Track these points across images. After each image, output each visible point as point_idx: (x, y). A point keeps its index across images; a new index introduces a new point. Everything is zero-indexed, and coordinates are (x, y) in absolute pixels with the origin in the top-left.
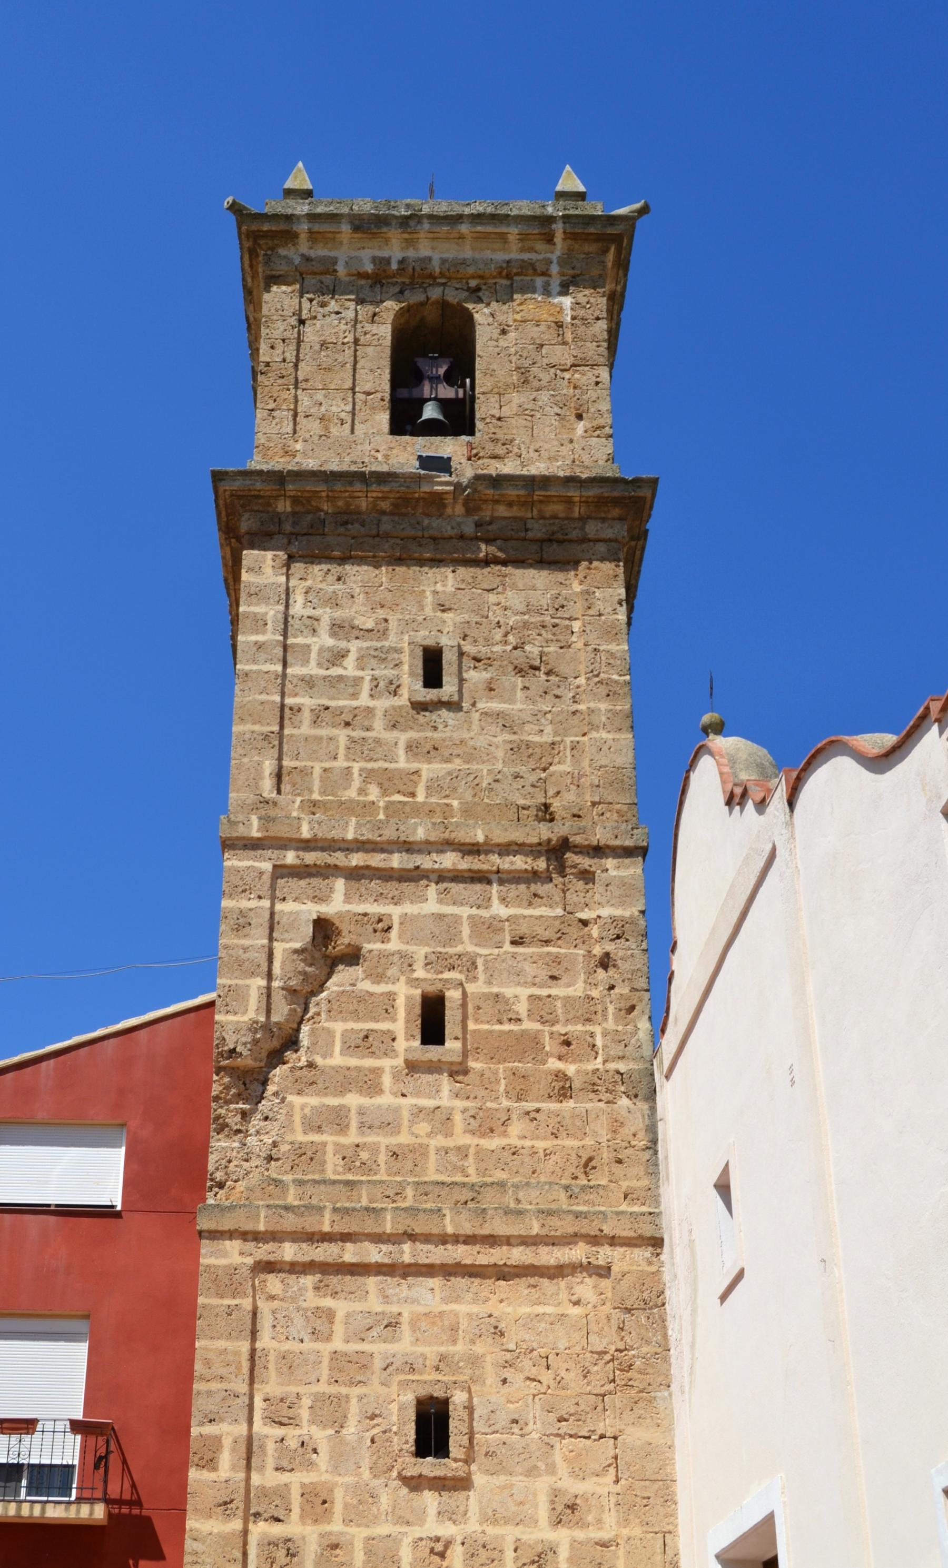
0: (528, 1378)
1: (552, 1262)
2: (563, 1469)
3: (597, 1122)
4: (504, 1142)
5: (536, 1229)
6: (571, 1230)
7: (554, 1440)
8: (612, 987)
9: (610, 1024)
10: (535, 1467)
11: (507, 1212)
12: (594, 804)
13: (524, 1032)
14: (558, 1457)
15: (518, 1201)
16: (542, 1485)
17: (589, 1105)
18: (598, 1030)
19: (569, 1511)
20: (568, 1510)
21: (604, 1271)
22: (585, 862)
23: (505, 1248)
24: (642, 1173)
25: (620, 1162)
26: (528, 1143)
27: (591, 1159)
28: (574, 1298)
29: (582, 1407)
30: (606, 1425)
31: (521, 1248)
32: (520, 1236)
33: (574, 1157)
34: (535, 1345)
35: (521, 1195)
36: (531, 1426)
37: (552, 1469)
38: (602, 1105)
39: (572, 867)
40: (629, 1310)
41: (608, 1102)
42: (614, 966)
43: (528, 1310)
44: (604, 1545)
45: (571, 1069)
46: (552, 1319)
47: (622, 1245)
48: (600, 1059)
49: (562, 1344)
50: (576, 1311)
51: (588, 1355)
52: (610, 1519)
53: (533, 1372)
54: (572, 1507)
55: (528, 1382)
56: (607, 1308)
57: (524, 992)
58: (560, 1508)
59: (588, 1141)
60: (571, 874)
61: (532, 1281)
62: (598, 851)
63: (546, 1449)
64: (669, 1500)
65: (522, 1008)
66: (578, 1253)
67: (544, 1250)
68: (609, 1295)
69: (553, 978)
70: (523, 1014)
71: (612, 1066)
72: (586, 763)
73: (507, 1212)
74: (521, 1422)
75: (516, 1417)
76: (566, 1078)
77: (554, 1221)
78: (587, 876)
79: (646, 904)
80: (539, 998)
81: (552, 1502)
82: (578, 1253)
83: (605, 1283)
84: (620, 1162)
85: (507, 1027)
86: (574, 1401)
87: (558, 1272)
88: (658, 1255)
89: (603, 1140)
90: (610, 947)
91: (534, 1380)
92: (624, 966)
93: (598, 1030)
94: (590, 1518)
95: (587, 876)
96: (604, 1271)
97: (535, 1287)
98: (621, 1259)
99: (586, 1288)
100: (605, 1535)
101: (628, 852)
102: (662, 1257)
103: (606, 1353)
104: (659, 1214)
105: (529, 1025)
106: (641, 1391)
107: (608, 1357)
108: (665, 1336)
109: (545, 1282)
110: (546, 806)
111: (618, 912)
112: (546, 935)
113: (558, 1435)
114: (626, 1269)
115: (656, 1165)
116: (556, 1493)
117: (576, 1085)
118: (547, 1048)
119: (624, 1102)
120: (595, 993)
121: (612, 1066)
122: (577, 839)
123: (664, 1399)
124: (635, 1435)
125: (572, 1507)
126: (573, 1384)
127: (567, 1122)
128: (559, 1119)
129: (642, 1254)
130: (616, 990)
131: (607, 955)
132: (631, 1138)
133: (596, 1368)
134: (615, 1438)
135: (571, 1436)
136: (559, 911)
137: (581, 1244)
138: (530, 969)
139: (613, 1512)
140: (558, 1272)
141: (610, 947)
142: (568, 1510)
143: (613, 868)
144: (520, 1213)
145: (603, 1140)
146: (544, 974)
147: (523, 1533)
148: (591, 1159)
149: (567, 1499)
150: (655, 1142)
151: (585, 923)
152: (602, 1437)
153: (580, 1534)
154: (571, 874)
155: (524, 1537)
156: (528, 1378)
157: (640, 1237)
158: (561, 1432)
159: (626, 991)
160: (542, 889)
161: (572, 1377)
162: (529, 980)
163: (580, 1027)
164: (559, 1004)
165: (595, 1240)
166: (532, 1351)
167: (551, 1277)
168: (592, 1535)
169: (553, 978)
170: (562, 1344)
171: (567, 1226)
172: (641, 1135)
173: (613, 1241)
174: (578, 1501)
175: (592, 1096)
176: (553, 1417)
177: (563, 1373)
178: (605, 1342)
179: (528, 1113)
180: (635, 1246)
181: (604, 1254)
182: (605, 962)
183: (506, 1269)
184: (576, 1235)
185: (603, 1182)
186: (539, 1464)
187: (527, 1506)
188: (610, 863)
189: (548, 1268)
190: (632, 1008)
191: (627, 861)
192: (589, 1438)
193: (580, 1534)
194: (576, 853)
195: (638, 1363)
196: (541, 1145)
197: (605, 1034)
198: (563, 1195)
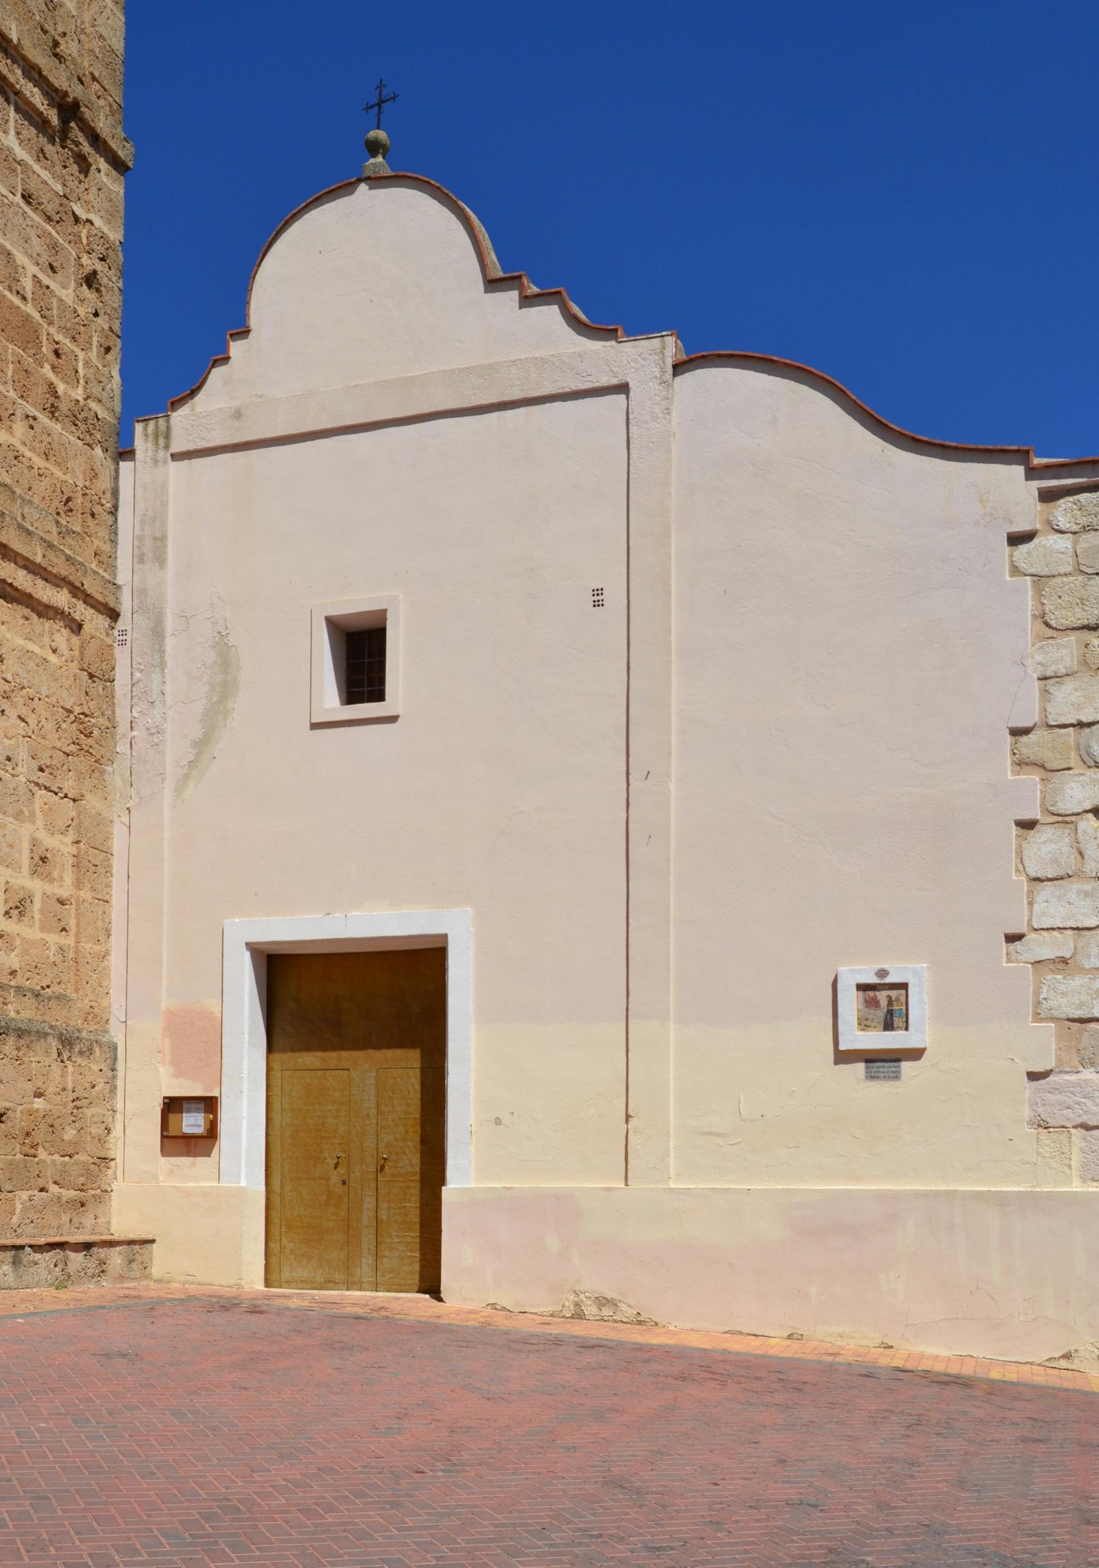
0: (19, 717)
1: (45, 600)
2: (40, 822)
3: (79, 462)
4: (11, 440)
5: (39, 559)
6: (64, 573)
7: (35, 789)
8: (96, 315)
9: (94, 355)
10: (21, 812)
11: (20, 527)
12: (94, 79)
13: (27, 318)
14: (37, 804)
15: (23, 517)
16: (26, 830)
17: (71, 438)
18: (81, 355)
19: (41, 863)
20: (42, 861)
21: (76, 627)
22: (86, 148)
23: (13, 565)
24: (107, 538)
25: (93, 515)
26: (28, 454)
27: (69, 500)
28: (54, 647)
29: (55, 762)
30: (69, 785)
31: (25, 572)
32: (27, 559)
33: (58, 491)
34: (26, 685)
35: (26, 510)
36: (19, 769)
37: (32, 819)
38: (80, 443)
39: (73, 141)
40: (91, 676)
41: (88, 444)
42: (98, 290)
43: (20, 641)
44: (62, 902)
45: (61, 388)
46: (37, 660)
47: (92, 606)
48: (80, 390)
49: (44, 691)
50: (53, 659)
51: (60, 710)
52: (69, 877)
53: (24, 711)
54: (43, 859)
55: (19, 721)
56: (74, 667)
57: (32, 269)
58: (37, 858)
59: (68, 478)
60: (70, 149)
61: (27, 612)
62: (95, 139)
63: (29, 795)
64: (108, 872)
65: (28, 285)
66: (61, 598)
67: (41, 583)
68: (77, 653)
69: (52, 267)
70: (29, 296)
71: (93, 405)
72: (87, 17)
73: (20, 527)
74: (13, 761)
75: (10, 754)
76: (55, 394)
77: (51, 555)
78: (84, 165)
79: (125, 236)
80: (39, 282)
81: (32, 851)
82: (61, 598)
83: (75, 639)
84: (93, 515)
85: (16, 301)
86: (49, 753)
87: (45, 611)
88: (113, 628)
89: (80, 484)
90: (99, 266)
91: (23, 720)
92: (107, 297)
93: (81, 355)
94: (56, 874)
95: (84, 165)
96: (76, 627)
97: (27, 619)
98: (94, 622)
99: (62, 637)
100: (64, 894)
101: (118, 165)
102: (116, 633)
103: (72, 712)
104: (119, 587)
105: (30, 309)
106: (96, 761)
107: (72, 717)
108: (113, 712)
109: (34, 616)
110: (56, 44)
111: (105, 229)
112: (50, 208)
113: (37, 784)
114: (94, 633)
115: (116, 534)
116: (35, 843)
117: (64, 407)
118: (44, 349)
119: (98, 451)
120: (81, 311)
121: (93, 405)
122: (87, 114)
123: (109, 774)
124: (92, 802)
125: (43, 859)
126: (49, 736)
127: (55, 446)
128: (49, 439)
129: (103, 621)
130: (99, 320)
131: (95, 272)
132: (101, 495)
133: (64, 726)
134: (74, 800)
135: (46, 788)
136: (59, 188)
137: (65, 591)
138: (37, 245)
139: (70, 873)
140: (45, 611)
141: (99, 266)
142: (42, 861)
143: (103, 173)
144: (29, 533)
145: (80, 484)
146: (45, 259)
147: (11, 876)
148: (69, 500)
149: (40, 851)
150: (116, 507)
151: (77, 219)
152: (66, 796)
153: (49, 889)
154: (70, 149)
155: (12, 881)
156: (19, 717)
157: (105, 605)
158: (40, 781)
159: (106, 327)
160: (49, 149)
161: (49, 726)
162: (35, 255)
163: (67, 341)
164: (55, 301)
165: (77, 591)
166: (23, 688)
167: (40, 615)
168: (56, 891)
169: (52, 267)
170: (44, 691)
171: (61, 568)
172: (108, 495)
173: (88, 599)
174: (48, 856)
175: (73, 428)
176: (35, 765)
177: (44, 721)
178: (72, 700)
179: (27, 416)
180: (99, 611)
181: (81, 611)
182: (90, 280)
183: (9, 589)
184: (63, 579)
185: (78, 529)
186: (25, 809)
187: (15, 850)
188: (103, 164)
189: (39, 602)
190: (108, 350)
191: (114, 173)
192: (56, 794)
193: (49, 889)
194: (81, 130)
195: (96, 732)
196: (38, 461)
197: (87, 364)
198: (55, 530)
